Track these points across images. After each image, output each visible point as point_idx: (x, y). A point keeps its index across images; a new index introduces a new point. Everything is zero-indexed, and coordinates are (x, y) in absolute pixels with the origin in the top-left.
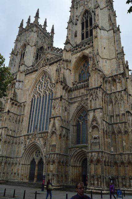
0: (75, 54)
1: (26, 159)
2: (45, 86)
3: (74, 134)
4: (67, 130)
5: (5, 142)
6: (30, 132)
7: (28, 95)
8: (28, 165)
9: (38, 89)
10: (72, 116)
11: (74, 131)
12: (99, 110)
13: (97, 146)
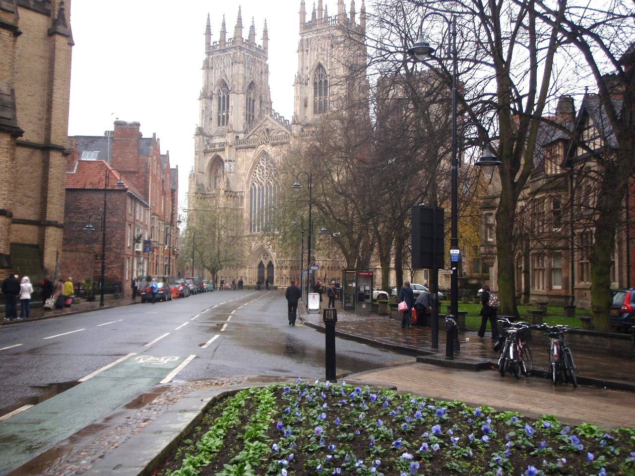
9: (257, 175)
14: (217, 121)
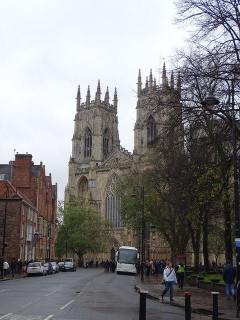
9: (110, 189)
14: (84, 154)
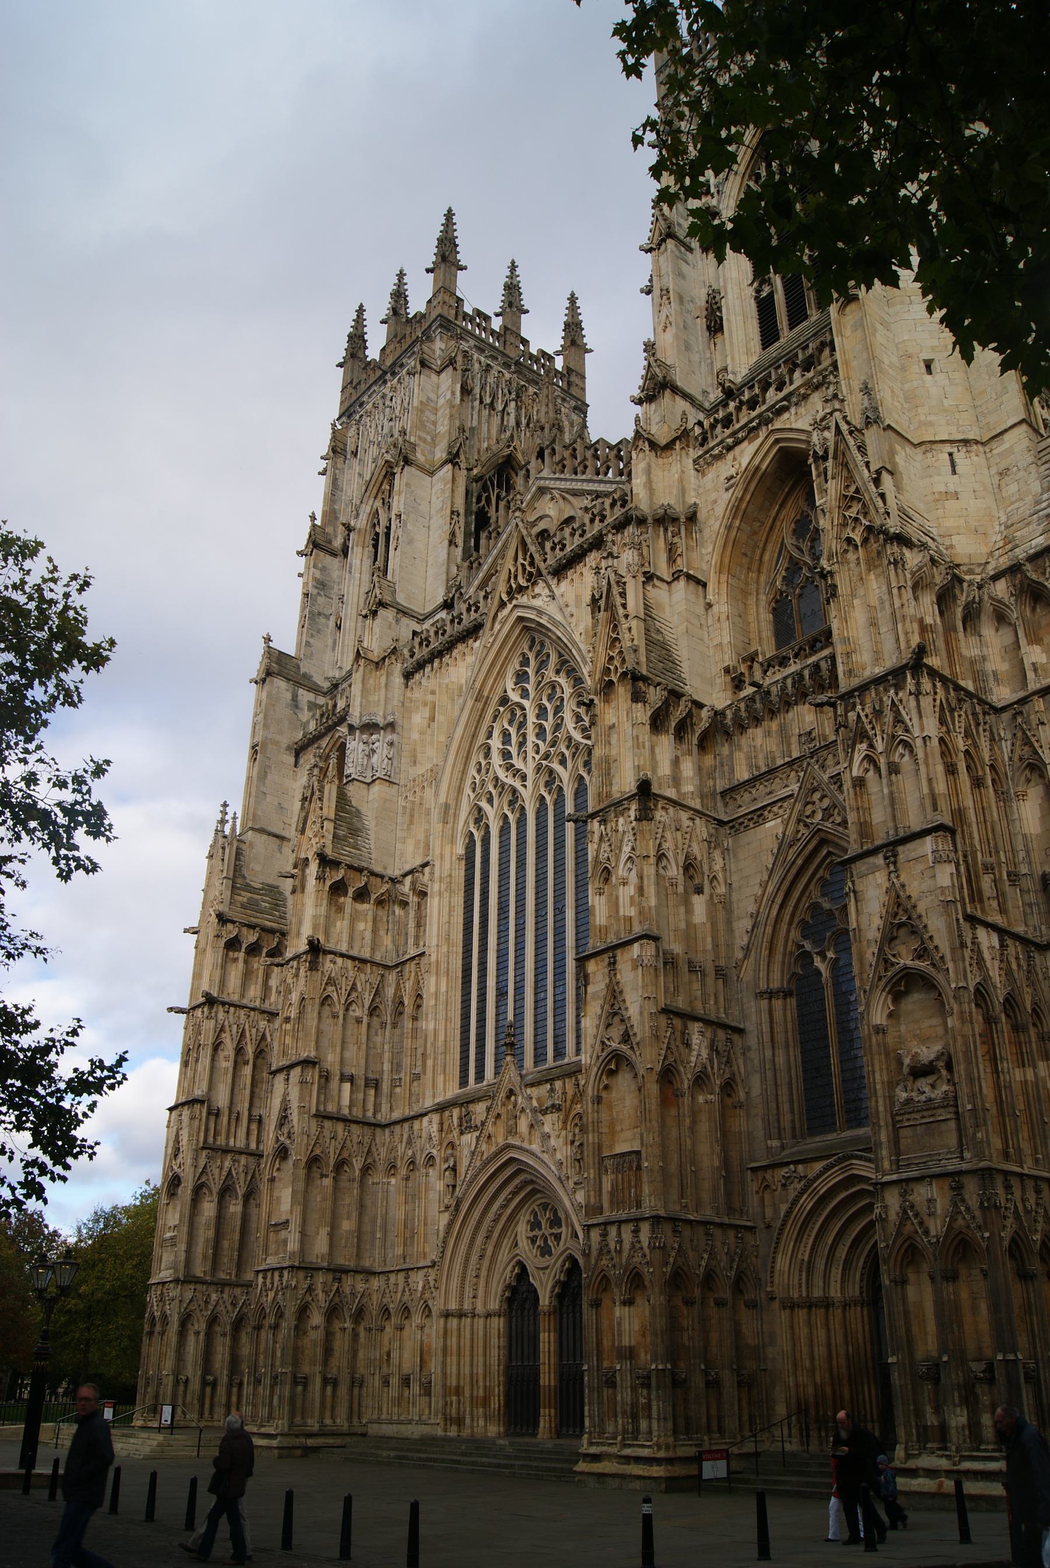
0: (720, 457)
1: (471, 1272)
2: (541, 733)
3: (781, 1059)
4: (721, 1034)
5: (313, 1162)
6: (480, 1076)
7: (435, 815)
8: (488, 1315)
9: (496, 759)
10: (746, 924)
11: (780, 1038)
12: (927, 845)
13: (943, 1127)
